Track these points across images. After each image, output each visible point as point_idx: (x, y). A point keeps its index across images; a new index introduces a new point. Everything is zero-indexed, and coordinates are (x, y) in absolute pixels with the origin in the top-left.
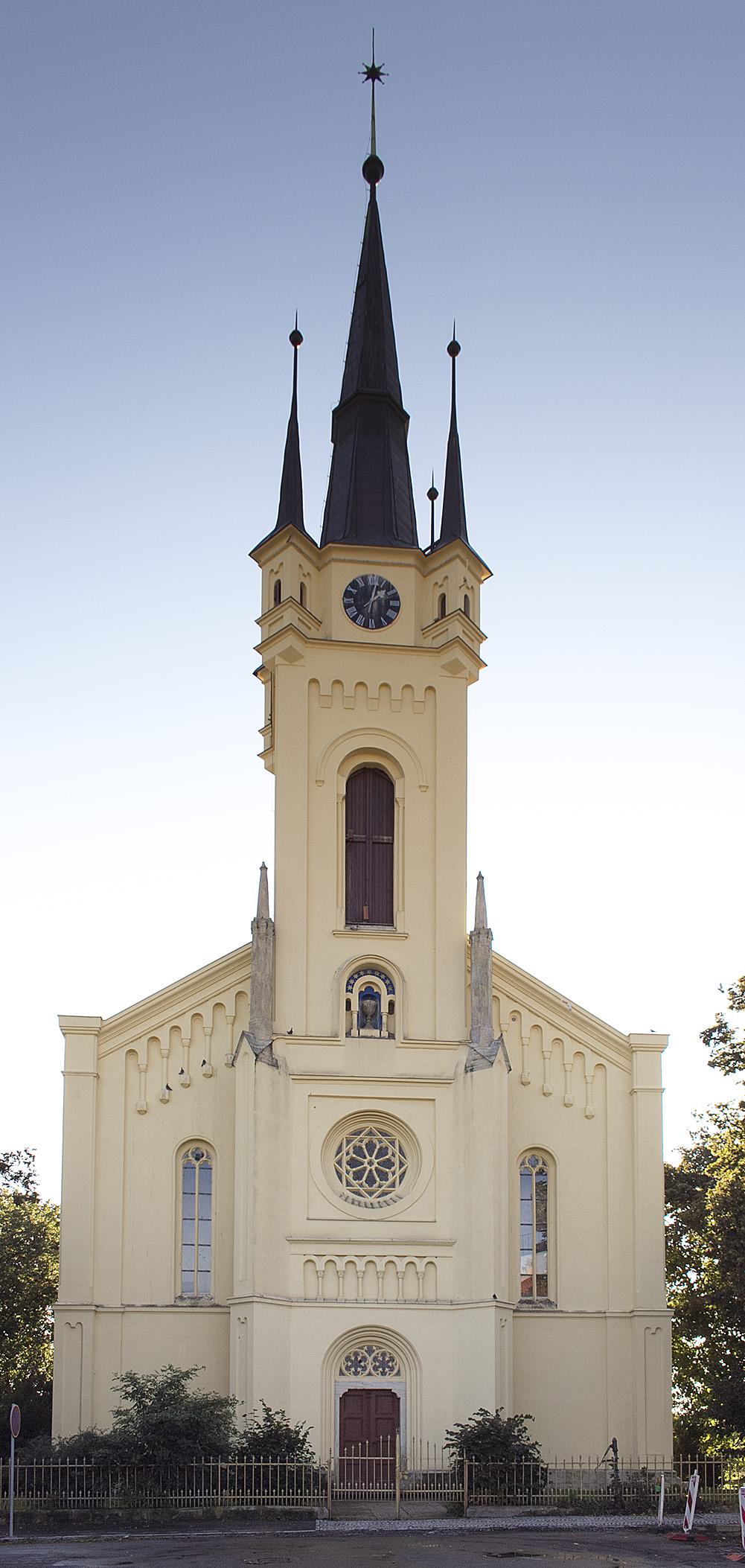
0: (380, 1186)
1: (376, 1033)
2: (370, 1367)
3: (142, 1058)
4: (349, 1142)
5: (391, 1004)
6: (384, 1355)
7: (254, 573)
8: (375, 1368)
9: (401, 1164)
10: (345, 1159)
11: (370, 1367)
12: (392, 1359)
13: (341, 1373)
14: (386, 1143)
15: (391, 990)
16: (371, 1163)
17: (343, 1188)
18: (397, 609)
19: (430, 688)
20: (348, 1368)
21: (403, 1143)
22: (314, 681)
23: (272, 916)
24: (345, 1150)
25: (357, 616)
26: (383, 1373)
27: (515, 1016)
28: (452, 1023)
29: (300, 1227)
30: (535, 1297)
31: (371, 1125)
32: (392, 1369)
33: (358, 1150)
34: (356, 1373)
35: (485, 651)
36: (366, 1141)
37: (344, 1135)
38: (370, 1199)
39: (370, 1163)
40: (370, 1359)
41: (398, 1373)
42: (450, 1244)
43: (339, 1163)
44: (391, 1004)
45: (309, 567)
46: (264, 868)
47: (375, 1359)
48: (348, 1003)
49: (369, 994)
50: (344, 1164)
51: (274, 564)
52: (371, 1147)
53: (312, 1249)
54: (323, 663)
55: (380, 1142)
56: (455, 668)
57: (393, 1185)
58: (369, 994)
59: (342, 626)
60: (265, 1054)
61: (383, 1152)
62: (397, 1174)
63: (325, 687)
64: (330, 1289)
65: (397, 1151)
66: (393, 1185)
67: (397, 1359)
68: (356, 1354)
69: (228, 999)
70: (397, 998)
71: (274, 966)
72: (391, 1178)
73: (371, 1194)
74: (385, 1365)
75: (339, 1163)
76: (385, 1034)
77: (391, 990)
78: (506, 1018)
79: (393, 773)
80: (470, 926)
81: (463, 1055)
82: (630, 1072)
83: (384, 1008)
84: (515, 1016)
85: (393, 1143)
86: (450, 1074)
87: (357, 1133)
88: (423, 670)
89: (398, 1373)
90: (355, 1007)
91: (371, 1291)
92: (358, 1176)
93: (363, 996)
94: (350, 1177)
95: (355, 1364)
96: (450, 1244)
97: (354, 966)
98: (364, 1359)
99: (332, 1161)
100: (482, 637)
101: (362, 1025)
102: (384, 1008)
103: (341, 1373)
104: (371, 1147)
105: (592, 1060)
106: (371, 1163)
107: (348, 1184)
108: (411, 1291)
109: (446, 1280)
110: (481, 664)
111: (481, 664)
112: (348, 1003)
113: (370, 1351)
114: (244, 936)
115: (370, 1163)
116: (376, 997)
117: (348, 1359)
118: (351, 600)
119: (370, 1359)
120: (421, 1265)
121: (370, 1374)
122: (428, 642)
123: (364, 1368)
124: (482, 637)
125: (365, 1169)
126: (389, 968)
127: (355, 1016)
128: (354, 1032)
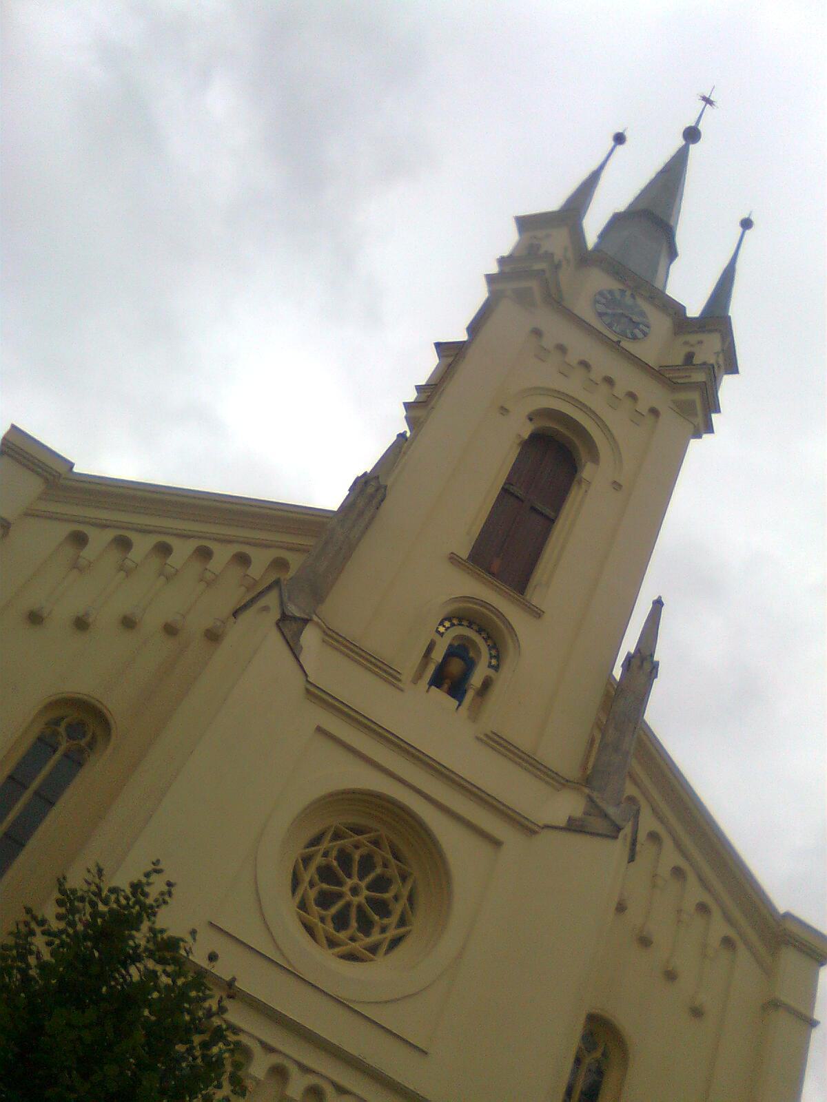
3: (88, 553)
4: (337, 836)
5: (487, 684)
9: (402, 922)
10: (318, 860)
14: (393, 872)
16: (355, 891)
19: (654, 412)
22: (537, 333)
24: (325, 845)
28: (563, 748)
33: (344, 859)
43: (306, 860)
44: (487, 684)
50: (312, 869)
52: (367, 864)
55: (385, 865)
56: (685, 410)
57: (373, 949)
58: (460, 652)
61: (381, 884)
62: (392, 933)
65: (405, 893)
72: (375, 937)
80: (629, 644)
85: (404, 878)
87: (358, 831)
88: (651, 394)
90: (438, 655)
93: (451, 653)
94: (312, 894)
97: (462, 605)
99: (297, 850)
101: (436, 681)
102: (476, 680)
104: (367, 864)
105: (719, 928)
107: (303, 906)
111: (709, 429)
114: (329, 495)
116: (470, 666)
118: (604, 301)
125: (340, 896)
126: (505, 631)
127: (431, 669)
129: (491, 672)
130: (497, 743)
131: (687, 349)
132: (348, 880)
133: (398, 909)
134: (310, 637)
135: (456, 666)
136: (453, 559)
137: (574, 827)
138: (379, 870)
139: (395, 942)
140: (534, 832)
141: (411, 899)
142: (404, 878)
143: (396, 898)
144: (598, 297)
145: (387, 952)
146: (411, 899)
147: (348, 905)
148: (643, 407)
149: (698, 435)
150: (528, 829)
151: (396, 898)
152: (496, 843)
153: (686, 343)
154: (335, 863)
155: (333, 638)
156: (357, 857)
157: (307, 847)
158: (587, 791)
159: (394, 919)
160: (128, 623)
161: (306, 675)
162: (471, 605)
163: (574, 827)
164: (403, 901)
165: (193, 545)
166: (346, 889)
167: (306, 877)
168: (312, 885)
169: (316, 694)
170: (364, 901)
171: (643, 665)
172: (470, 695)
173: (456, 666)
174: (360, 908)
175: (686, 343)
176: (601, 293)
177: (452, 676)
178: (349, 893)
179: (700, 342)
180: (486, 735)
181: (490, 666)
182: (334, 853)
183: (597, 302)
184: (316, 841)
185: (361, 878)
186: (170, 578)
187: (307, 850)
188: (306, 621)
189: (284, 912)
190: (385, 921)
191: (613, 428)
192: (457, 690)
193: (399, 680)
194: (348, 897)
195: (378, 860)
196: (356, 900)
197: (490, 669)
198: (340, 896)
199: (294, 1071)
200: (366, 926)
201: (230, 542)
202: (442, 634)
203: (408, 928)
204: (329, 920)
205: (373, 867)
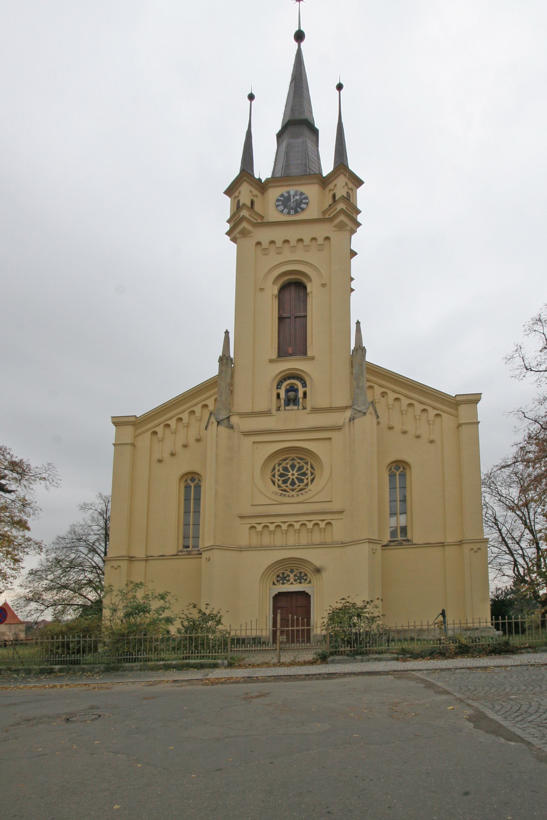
0: (299, 486)
1: (296, 407)
2: (292, 580)
5: (305, 394)
6: (300, 573)
7: (227, 200)
8: (295, 580)
9: (312, 474)
10: (277, 474)
11: (292, 580)
12: (306, 575)
13: (274, 584)
14: (302, 463)
15: (304, 385)
16: (293, 475)
17: (276, 489)
18: (307, 204)
19: (327, 238)
21: (312, 462)
22: (259, 243)
23: (232, 356)
24: (277, 468)
25: (283, 210)
26: (300, 583)
27: (384, 394)
29: (248, 510)
30: (399, 538)
31: (293, 456)
33: (285, 469)
34: (283, 583)
35: (360, 218)
36: (290, 464)
37: (276, 461)
38: (292, 493)
39: (293, 475)
40: (292, 576)
41: (310, 582)
42: (341, 512)
44: (305, 394)
45: (255, 192)
46: (227, 333)
47: (295, 575)
48: (278, 396)
49: (292, 389)
50: (277, 476)
51: (236, 194)
52: (293, 467)
53: (254, 521)
54: (264, 235)
55: (299, 463)
56: (341, 227)
57: (307, 485)
58: (292, 389)
59: (274, 215)
60: (225, 421)
63: (265, 245)
64: (266, 540)
65: (309, 467)
66: (307, 485)
68: (283, 574)
69: (210, 403)
70: (308, 389)
71: (232, 377)
72: (305, 482)
73: (293, 490)
74: (301, 578)
75: (274, 476)
76: (301, 407)
77: (304, 385)
78: (378, 395)
79: (304, 280)
81: (348, 413)
82: (457, 416)
83: (301, 395)
84: (384, 394)
85: (307, 463)
86: (340, 423)
88: (321, 231)
89: (310, 582)
91: (291, 539)
93: (287, 391)
94: (280, 483)
95: (283, 579)
96: (341, 512)
98: (288, 576)
100: (358, 212)
102: (301, 395)
103: (274, 584)
104: (293, 467)
106: (293, 475)
107: (279, 486)
108: (317, 537)
109: (339, 530)
110: (358, 225)
111: (358, 225)
112: (278, 396)
115: (293, 475)
117: (278, 576)
119: (292, 576)
120: (322, 525)
121: (292, 583)
122: (327, 216)
123: (288, 581)
124: (358, 212)
127: (283, 401)
128: (282, 408)
129: (304, 389)
131: (332, 193)
133: (309, 472)
136: (271, 361)
138: (297, 466)
139: (312, 480)
141: (312, 467)
142: (307, 463)
143: (307, 469)
144: (277, 203)
146: (312, 467)
147: (293, 479)
148: (320, 241)
149: (353, 232)
151: (307, 469)
153: (330, 190)
156: (288, 466)
157: (272, 471)
168: (279, 480)
171: (360, 350)
173: (292, 394)
175: (330, 190)
176: (278, 200)
179: (335, 185)
181: (303, 387)
182: (281, 469)
183: (277, 206)
184: (274, 469)
185: (293, 470)
190: (307, 477)
191: (312, 263)
194: (292, 477)
196: (294, 477)
198: (289, 478)
204: (289, 485)
205: (295, 466)
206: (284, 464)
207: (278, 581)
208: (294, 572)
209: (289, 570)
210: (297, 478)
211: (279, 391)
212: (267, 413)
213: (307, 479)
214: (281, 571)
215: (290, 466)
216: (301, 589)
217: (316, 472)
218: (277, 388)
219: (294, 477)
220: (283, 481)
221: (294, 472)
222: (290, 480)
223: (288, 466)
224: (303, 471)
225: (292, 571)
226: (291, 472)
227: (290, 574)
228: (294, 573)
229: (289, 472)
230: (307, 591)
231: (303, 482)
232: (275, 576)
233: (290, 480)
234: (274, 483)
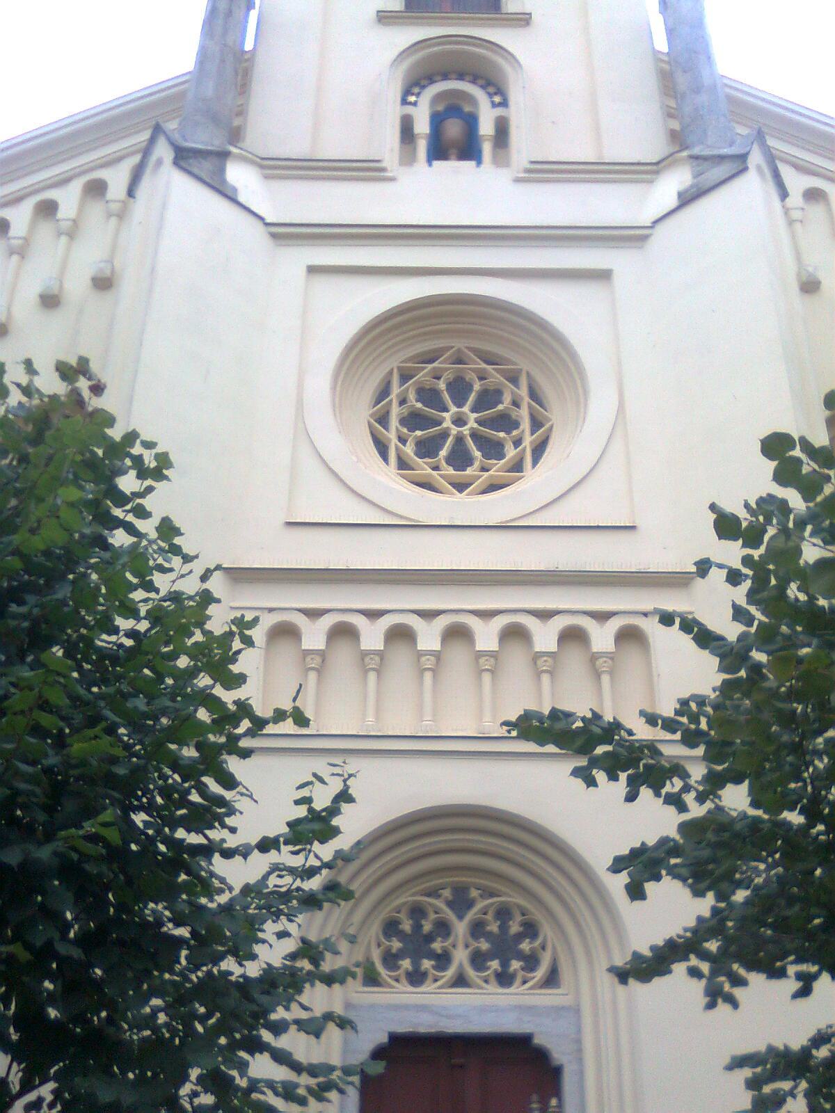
2: (461, 956)
6: (503, 914)
8: (478, 960)
9: (536, 424)
10: (396, 412)
11: (461, 956)
12: (530, 930)
20: (391, 960)
24: (396, 390)
26: (504, 979)
32: (531, 962)
33: (429, 396)
34: (417, 978)
36: (448, 376)
40: (461, 928)
41: (552, 979)
47: (477, 929)
50: (394, 422)
57: (518, 467)
61: (488, 398)
62: (528, 441)
65: (523, 392)
67: (547, 930)
68: (417, 912)
72: (511, 452)
74: (510, 948)
75: (383, 420)
85: (514, 380)
89: (552, 979)
90: (422, 126)
92: (427, 448)
94: (409, 449)
98: (443, 928)
99: (363, 412)
102: (486, 127)
106: (459, 421)
107: (403, 464)
113: (461, 903)
116: (471, 122)
117: (391, 928)
119: (461, 928)
121: (460, 981)
123: (443, 960)
129: (499, 111)
130: (545, 172)
132: (444, 414)
133: (524, 415)
134: (238, 175)
135: (453, 129)
137: (687, 199)
139: (539, 450)
140: (644, 238)
141: (534, 395)
142: (514, 380)
143: (516, 404)
145: (535, 461)
146: (534, 395)
147: (460, 440)
150: (632, 237)
151: (516, 404)
152: (603, 276)
154: (419, 405)
155: (276, 168)
156: (442, 385)
157: (378, 402)
158: (685, 154)
159: (526, 425)
160: (50, 301)
161: (261, 219)
162: (436, 49)
163: (687, 199)
164: (526, 399)
165: (76, 187)
166: (447, 424)
167: (392, 436)
168: (403, 440)
169: (285, 234)
170: (475, 425)
172: (487, 148)
174: (474, 435)
177: (454, 139)
178: (453, 427)
180: (528, 171)
181: (494, 105)
182: (412, 396)
184: (384, 392)
186: (72, 232)
187: (375, 408)
188: (224, 155)
189: (391, 489)
192: (468, 150)
193: (383, 170)
194: (454, 430)
195: (471, 377)
196: (465, 430)
197: (495, 110)
199: (473, 623)
200: (493, 449)
201: (120, 159)
202: (415, 104)
203: (547, 426)
205: (469, 387)
206: (423, 375)
207: (391, 960)
208: (470, 904)
209: (447, 893)
210: (474, 435)
211: (409, 110)
212: (366, 170)
213: (517, 443)
214: (405, 898)
215: (450, 386)
216: (508, 1024)
217: (555, 415)
218: (404, 102)
219: (465, 430)
220: (450, 460)
221: (466, 409)
222: (450, 442)
223: (442, 385)
224: (500, 407)
225: (461, 903)
226: (454, 409)
227: (450, 915)
228: (471, 915)
229: (446, 410)
230: (547, 1035)
231: (500, 455)
232: (375, 929)
233: (450, 442)
234: (382, 448)
